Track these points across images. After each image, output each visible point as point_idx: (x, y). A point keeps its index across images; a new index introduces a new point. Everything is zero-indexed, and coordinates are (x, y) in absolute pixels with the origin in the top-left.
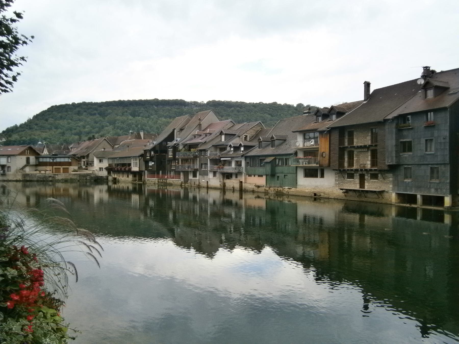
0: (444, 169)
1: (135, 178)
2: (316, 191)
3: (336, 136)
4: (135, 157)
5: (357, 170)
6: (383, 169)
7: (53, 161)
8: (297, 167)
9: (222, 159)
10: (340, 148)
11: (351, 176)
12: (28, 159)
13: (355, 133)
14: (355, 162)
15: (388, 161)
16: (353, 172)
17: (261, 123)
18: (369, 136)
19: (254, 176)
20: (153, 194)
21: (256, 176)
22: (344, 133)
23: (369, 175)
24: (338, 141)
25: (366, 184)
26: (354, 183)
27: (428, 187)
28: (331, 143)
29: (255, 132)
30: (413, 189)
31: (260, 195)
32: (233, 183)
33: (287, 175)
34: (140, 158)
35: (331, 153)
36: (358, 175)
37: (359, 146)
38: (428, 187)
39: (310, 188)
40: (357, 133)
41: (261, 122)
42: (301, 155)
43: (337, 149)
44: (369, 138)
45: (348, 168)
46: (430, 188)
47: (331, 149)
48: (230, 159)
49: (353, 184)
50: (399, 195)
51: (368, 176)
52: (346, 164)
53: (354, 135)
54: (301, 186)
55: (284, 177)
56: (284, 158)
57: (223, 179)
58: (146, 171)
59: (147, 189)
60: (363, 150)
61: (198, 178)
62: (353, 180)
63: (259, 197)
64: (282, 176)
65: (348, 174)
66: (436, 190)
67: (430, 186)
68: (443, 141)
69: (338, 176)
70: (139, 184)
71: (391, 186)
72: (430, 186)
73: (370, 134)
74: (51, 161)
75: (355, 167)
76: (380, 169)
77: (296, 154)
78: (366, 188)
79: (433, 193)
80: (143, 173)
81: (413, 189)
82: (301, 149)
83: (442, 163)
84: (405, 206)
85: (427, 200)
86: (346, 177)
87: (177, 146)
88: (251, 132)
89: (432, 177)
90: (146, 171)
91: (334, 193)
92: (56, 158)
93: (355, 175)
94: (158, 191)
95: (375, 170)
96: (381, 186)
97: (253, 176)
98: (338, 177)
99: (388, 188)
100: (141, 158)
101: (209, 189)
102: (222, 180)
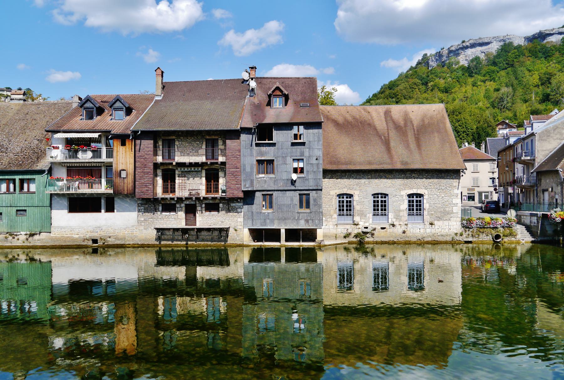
0: (316, 195)
2: (95, 235)
5: (180, 200)
6: (236, 196)
8: (51, 195)
13: (177, 143)
15: (245, 185)
16: (173, 202)
23: (204, 206)
26: (175, 218)
27: (296, 218)
28: (137, 155)
30: (276, 222)
33: (25, 211)
35: (138, 170)
36: (183, 205)
37: (193, 164)
38: (296, 218)
39: (84, 231)
42: (62, 173)
44: (203, 151)
45: (163, 195)
46: (298, 219)
47: (137, 165)
49: (174, 219)
50: (252, 231)
51: (202, 208)
53: (176, 146)
54: (62, 228)
56: (17, 178)
62: (174, 213)
65: (162, 204)
66: (307, 221)
67: (298, 217)
68: (315, 162)
69: (142, 208)
71: (241, 220)
72: (298, 217)
73: (204, 147)
76: (231, 196)
77: (50, 171)
78: (199, 225)
79: (302, 225)
81: (276, 222)
82: (61, 164)
83: (315, 188)
84: (261, 246)
85: (292, 235)
86: (160, 208)
89: (301, 206)
91: (136, 237)
93: (178, 206)
95: (213, 198)
96: (223, 221)
98: (143, 210)
99: (234, 222)
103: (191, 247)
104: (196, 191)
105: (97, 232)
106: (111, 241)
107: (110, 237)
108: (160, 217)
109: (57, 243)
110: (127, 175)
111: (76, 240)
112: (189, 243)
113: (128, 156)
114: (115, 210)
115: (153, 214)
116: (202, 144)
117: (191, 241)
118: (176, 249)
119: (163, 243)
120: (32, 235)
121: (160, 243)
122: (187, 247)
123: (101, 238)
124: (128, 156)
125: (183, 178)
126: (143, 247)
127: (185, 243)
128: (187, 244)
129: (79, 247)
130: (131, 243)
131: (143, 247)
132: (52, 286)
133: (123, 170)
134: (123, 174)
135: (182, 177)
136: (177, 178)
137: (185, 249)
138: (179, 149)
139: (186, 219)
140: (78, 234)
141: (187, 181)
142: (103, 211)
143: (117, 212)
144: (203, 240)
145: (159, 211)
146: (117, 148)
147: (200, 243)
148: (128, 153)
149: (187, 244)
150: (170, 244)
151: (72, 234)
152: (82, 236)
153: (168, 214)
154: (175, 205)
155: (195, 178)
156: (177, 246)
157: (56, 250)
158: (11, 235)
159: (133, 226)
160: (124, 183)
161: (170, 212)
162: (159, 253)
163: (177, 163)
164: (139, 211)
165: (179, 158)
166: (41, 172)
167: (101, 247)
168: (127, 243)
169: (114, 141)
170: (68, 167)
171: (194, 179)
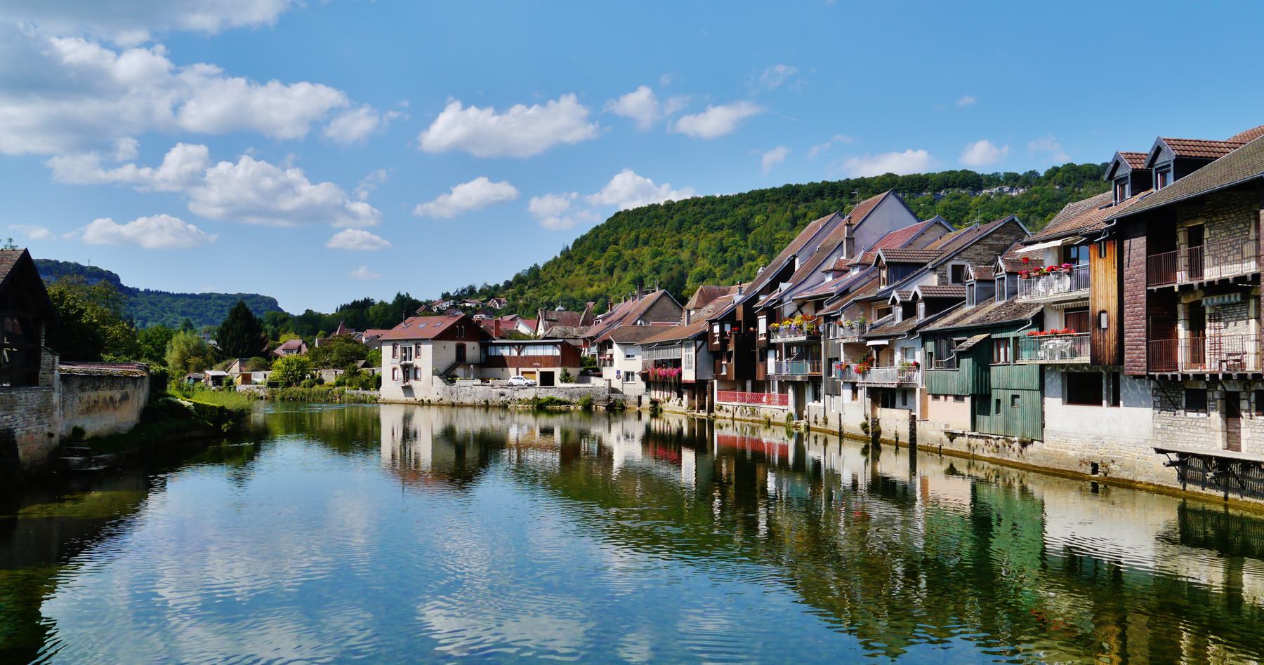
1: (692, 401)
2: (1096, 455)
3: (1137, 247)
4: (684, 343)
7: (519, 353)
8: (1042, 367)
9: (870, 343)
10: (1149, 293)
11: (1197, 402)
12: (461, 350)
13: (1206, 234)
14: (1207, 345)
16: (1202, 386)
17: (1016, 223)
18: (1248, 240)
19: (946, 396)
20: (733, 451)
21: (950, 399)
22: (1175, 238)
23: (1253, 397)
24: (1143, 267)
25: (1245, 433)
26: (1206, 428)
28: (1126, 274)
29: (993, 252)
31: (961, 465)
32: (893, 421)
34: (699, 343)
35: (1127, 311)
36: (1217, 396)
40: (1213, 232)
41: (1017, 219)
42: (1055, 322)
43: (1143, 295)
47: (1126, 298)
48: (886, 342)
49: (1203, 431)
52: (1182, 355)
53: (1205, 241)
55: (1013, 403)
56: (1011, 335)
57: (873, 409)
58: (715, 381)
59: (719, 438)
60: (1233, 299)
61: (822, 401)
62: (1203, 415)
63: (952, 471)
64: (1005, 397)
65: (1187, 391)
70: (702, 421)
74: (515, 353)
75: (1210, 366)
78: (1245, 453)
80: (709, 386)
86: (1184, 404)
87: (774, 305)
88: (980, 254)
90: (715, 381)
92: (525, 345)
93: (1209, 395)
94: (743, 440)
97: (942, 398)
100: (702, 344)
101: (845, 441)
102: (869, 411)
103: (1236, 508)
104: (1239, 357)
105: (1097, 449)
106: (1116, 471)
107: (1113, 462)
108: (1183, 423)
109: (1050, 464)
110: (1108, 323)
111: (1069, 461)
112: (1231, 496)
113: (1109, 280)
114: (1121, 402)
115: (1175, 414)
116: (1249, 227)
117: (1235, 491)
118: (1208, 507)
119: (1190, 487)
120: (1024, 444)
121: (1184, 490)
122: (1226, 507)
123: (1102, 462)
124: (1109, 280)
125: (1217, 324)
126: (1160, 493)
127: (1221, 494)
128: (1226, 498)
129: (1075, 476)
130: (1144, 480)
131: (1161, 490)
132: (1044, 549)
133: (1104, 312)
134: (1104, 325)
135: (1215, 321)
136: (1208, 324)
137: (1222, 509)
138: (1212, 248)
139: (1228, 432)
140: (1074, 450)
141: (1224, 332)
142: (1104, 402)
143: (1125, 405)
144: (1253, 494)
145: (1182, 409)
146: (1094, 262)
147: (1248, 499)
148: (1109, 272)
149: (1226, 498)
150: (1198, 493)
151: (1067, 448)
152: (1079, 453)
153: (1194, 415)
154: (1204, 391)
155: (1238, 323)
156: (1209, 499)
157: (1051, 479)
158: (1008, 441)
159: (1146, 441)
160: (1104, 342)
161: (1197, 411)
162: (1183, 511)
163: (1180, 287)
164: (1155, 407)
165: (1211, 273)
166: (1022, 323)
167: (1103, 482)
168: (1138, 480)
169: (1090, 248)
170: (1066, 310)
171: (1235, 325)
